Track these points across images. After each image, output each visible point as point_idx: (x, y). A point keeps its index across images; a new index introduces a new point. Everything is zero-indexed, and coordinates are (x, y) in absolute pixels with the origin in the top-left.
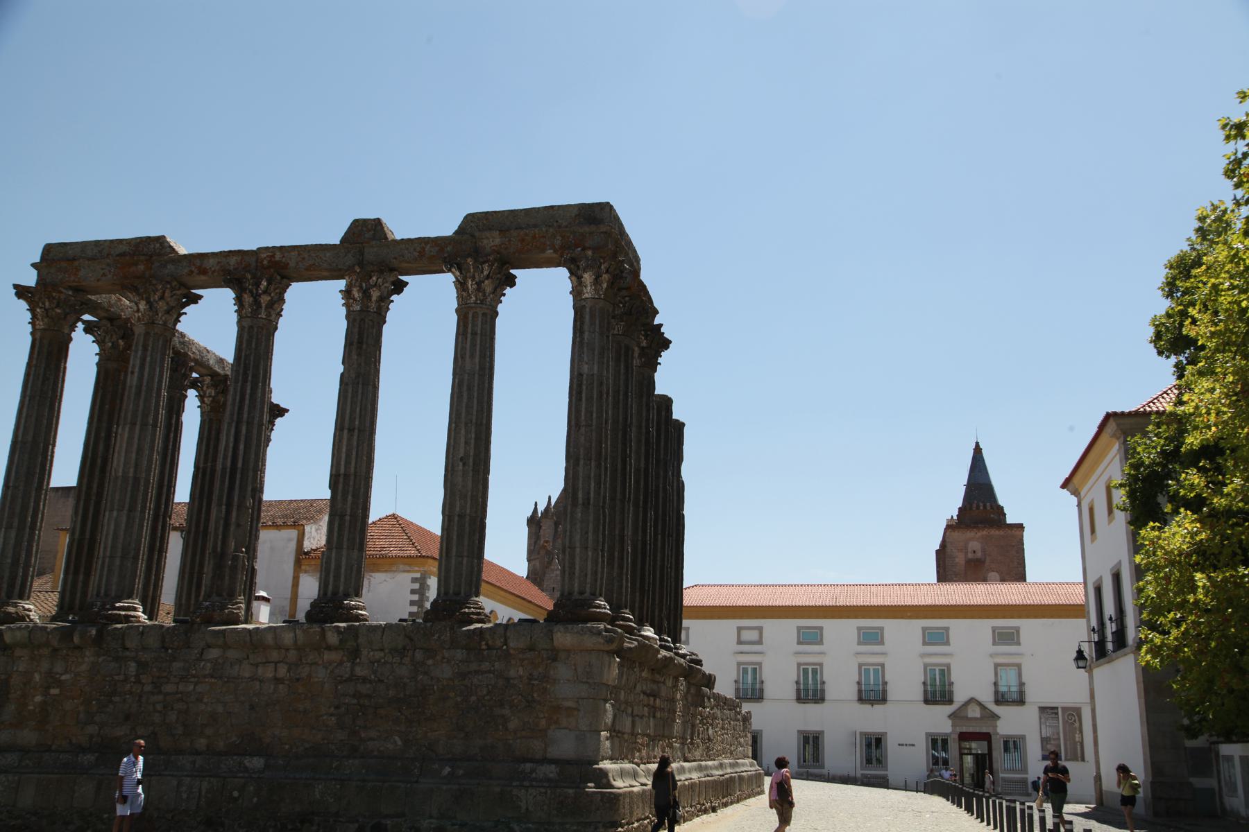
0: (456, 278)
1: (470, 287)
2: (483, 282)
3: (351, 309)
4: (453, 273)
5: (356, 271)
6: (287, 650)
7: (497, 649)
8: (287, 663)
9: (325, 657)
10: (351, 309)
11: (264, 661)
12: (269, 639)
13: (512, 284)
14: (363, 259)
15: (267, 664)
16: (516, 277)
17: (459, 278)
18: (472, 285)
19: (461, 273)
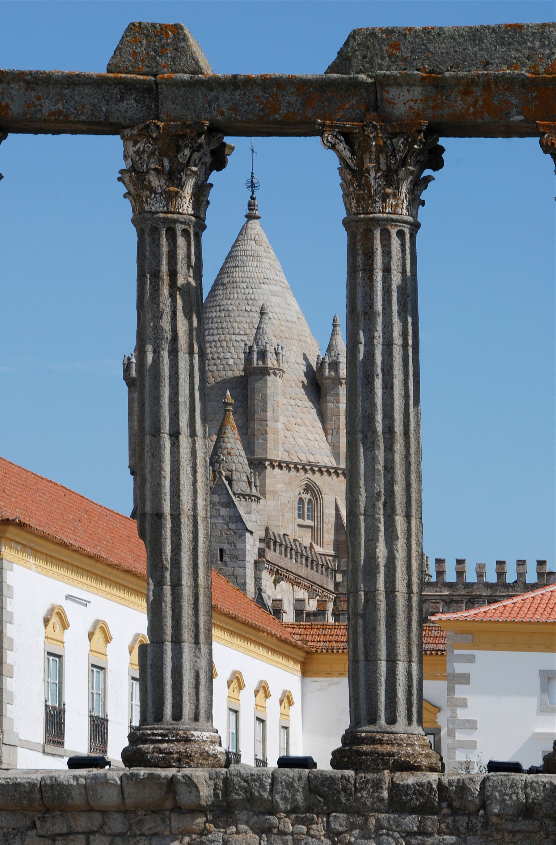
0: (342, 159)
1: (372, 182)
2: (396, 172)
3: (147, 208)
4: (337, 151)
5: (151, 136)
6: (104, 812)
7: (470, 815)
8: (104, 834)
9: (174, 824)
10: (147, 208)
11: (65, 830)
12: (78, 799)
13: (438, 164)
14: (157, 106)
15: (71, 837)
16: (442, 150)
17: (349, 162)
18: (375, 178)
19: (353, 153)
